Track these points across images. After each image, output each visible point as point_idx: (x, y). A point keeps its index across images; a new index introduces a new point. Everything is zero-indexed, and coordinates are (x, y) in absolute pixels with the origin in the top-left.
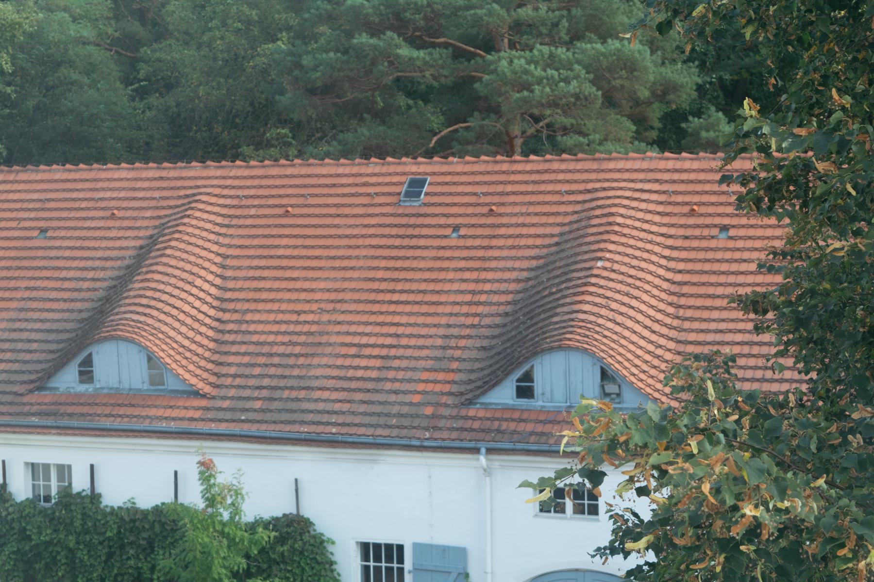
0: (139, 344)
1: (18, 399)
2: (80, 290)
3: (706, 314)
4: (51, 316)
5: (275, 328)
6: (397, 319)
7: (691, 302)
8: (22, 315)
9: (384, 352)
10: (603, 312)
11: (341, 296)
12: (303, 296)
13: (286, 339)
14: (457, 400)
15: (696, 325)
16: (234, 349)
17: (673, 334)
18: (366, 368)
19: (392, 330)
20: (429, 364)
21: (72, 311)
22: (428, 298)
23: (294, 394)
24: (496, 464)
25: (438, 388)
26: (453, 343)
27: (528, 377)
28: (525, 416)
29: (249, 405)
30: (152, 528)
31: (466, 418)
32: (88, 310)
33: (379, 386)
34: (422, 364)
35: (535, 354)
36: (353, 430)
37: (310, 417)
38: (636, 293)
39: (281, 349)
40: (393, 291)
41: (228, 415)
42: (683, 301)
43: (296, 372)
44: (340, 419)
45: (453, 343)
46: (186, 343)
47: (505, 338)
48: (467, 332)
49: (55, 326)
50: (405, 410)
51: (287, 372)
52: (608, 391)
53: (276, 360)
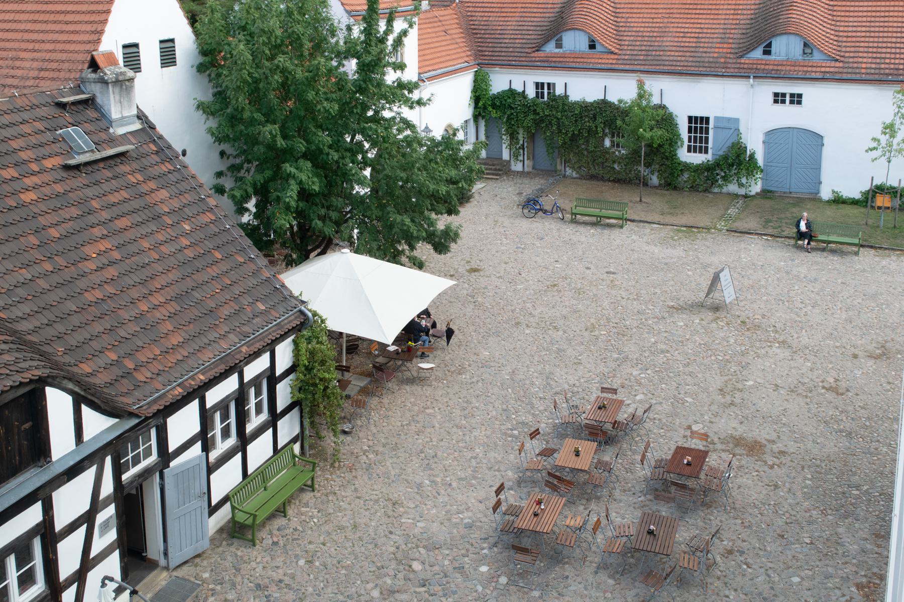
0: (585, 32)
1: (528, 55)
2: (547, 8)
3: (847, 19)
4: (535, 19)
5: (643, 25)
6: (700, 21)
7: (839, 14)
8: (522, 19)
9: (696, 35)
10: (802, 18)
11: (672, 11)
12: (654, 11)
13: (649, 29)
14: (735, 56)
15: (842, 24)
16: (625, 34)
17: (832, 27)
18: (689, 42)
19: (699, 26)
20: (719, 40)
21: (545, 17)
22: (713, 12)
23: (658, 53)
24: (756, 83)
25: (725, 51)
26: (728, 31)
27: (769, 45)
28: (768, 63)
29: (637, 58)
30: (596, 110)
31: (740, 63)
32: (552, 17)
33: (697, 50)
34: (715, 40)
35: (774, 36)
36: (689, 68)
37: (667, 63)
38: (815, 10)
39: (648, 34)
40: (696, 9)
41: (629, 62)
42: (835, 13)
43: (656, 44)
44: (682, 64)
45: (728, 31)
46: (604, 31)
47: (753, 29)
48: (734, 27)
49: (539, 24)
50: (711, 60)
51: (653, 44)
52: (806, 52)
53: (646, 39)
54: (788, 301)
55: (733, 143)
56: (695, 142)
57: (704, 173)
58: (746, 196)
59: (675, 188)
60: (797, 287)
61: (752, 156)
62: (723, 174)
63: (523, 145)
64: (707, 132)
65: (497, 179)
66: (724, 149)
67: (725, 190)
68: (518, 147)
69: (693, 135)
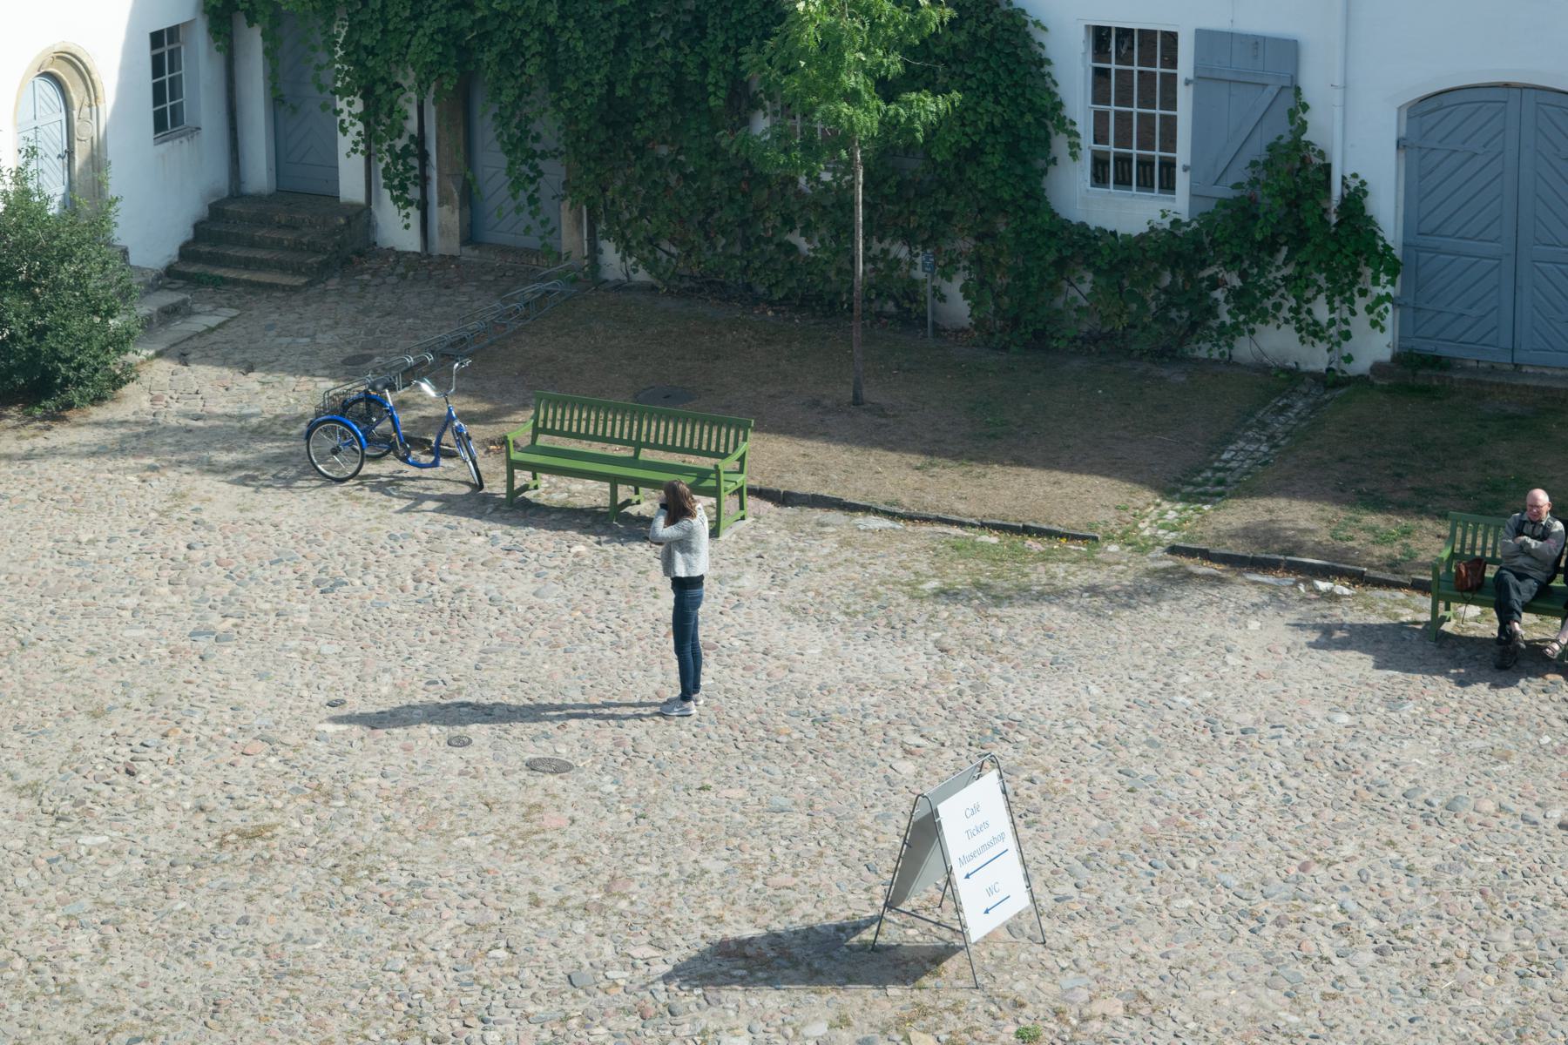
54: (1279, 923)
55: (1270, 148)
56: (1123, 139)
57: (1157, 274)
58: (1330, 381)
59: (1040, 340)
60: (1349, 849)
61: (1355, 200)
62: (1237, 282)
63: (420, 140)
64: (1170, 102)
65: (294, 289)
66: (1240, 174)
67: (1244, 349)
68: (400, 144)
69: (1112, 108)
